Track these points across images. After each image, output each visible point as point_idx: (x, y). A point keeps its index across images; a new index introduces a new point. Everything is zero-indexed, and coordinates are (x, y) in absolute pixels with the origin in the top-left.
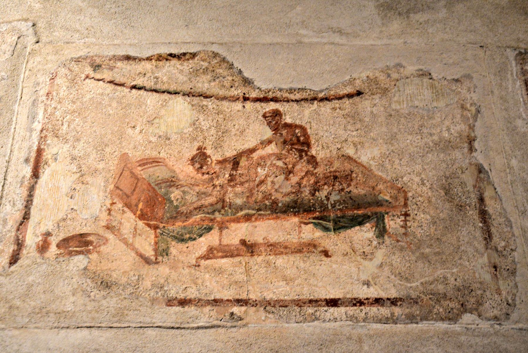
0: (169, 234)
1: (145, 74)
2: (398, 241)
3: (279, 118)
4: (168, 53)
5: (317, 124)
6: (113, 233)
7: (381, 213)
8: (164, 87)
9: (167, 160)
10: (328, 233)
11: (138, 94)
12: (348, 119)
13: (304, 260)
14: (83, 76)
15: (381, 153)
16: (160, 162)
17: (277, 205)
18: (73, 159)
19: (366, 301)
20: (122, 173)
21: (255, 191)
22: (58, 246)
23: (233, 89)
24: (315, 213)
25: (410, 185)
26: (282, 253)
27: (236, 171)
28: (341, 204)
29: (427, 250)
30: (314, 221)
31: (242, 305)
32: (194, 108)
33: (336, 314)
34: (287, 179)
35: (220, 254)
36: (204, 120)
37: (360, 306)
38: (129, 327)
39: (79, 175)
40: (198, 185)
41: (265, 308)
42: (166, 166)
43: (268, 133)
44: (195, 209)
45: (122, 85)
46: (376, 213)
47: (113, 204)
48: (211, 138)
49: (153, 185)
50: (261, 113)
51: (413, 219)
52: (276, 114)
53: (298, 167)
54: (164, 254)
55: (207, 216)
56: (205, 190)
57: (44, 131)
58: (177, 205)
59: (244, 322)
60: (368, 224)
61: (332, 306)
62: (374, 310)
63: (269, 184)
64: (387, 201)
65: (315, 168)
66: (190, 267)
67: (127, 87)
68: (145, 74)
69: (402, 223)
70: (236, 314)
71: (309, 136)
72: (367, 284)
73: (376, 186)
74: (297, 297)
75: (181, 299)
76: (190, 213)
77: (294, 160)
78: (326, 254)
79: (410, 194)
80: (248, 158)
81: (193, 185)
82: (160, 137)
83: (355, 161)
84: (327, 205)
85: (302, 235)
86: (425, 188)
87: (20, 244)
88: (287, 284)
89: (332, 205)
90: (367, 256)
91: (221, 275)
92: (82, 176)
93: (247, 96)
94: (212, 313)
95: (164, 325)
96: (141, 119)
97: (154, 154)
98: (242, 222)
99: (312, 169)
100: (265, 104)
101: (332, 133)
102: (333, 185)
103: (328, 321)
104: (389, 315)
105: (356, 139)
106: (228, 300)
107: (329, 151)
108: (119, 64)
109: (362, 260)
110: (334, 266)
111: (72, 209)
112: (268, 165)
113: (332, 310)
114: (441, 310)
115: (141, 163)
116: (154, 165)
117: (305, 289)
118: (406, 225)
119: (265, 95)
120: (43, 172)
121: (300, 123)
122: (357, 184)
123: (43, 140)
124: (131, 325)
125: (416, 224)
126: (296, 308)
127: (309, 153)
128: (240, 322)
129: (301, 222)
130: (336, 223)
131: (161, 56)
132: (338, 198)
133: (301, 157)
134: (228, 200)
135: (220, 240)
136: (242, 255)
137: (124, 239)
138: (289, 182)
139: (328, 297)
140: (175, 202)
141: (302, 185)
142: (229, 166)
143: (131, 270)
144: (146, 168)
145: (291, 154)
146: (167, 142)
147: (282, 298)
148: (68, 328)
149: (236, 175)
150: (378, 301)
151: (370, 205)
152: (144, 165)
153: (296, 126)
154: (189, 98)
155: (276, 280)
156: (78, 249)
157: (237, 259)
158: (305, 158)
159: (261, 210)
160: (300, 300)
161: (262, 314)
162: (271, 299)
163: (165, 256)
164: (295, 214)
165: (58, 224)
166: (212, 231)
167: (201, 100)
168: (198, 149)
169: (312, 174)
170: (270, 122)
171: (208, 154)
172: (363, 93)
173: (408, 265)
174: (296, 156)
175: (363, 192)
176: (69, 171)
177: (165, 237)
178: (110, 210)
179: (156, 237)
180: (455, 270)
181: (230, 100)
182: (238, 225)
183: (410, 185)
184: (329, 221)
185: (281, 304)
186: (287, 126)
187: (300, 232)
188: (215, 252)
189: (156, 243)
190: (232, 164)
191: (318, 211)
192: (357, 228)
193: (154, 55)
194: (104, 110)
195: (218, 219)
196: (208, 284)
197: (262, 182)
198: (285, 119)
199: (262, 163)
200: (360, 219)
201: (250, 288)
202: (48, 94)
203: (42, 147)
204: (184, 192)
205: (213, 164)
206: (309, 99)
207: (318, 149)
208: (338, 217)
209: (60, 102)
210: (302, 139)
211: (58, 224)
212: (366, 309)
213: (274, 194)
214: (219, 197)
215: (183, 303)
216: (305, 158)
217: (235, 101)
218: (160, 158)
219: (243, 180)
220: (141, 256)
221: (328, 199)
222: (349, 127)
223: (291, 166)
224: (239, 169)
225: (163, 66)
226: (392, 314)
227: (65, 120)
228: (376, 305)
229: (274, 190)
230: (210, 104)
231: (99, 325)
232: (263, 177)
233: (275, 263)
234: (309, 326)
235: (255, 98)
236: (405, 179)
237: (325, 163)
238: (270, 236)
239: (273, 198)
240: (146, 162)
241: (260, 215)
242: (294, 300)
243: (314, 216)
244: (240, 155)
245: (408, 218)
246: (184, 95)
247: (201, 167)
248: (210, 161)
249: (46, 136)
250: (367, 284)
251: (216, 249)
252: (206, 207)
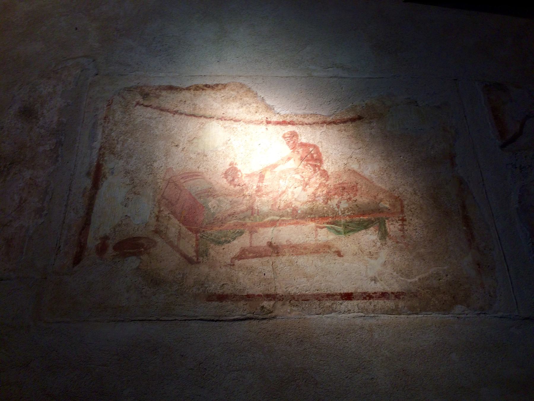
0: (208, 237)
1: (185, 102)
2: (397, 242)
4: (204, 84)
6: (161, 237)
9: (205, 174)
10: (340, 235)
12: (352, 139)
13: (321, 260)
14: (134, 103)
15: (380, 167)
17: (297, 212)
18: (127, 172)
19: (374, 295)
20: (168, 184)
21: (278, 201)
22: (115, 248)
23: (257, 114)
24: (328, 218)
25: (405, 194)
26: (302, 254)
27: (262, 182)
28: (349, 211)
29: (422, 250)
30: (328, 225)
31: (271, 300)
32: (226, 129)
33: (350, 307)
34: (304, 190)
35: (251, 255)
37: (370, 299)
38: (176, 320)
39: (131, 186)
40: (231, 195)
41: (290, 302)
42: (204, 178)
43: (287, 151)
44: (229, 215)
45: (168, 111)
46: (378, 219)
47: (160, 211)
49: (194, 195)
50: (281, 134)
51: (409, 223)
52: (294, 135)
53: (313, 180)
54: (204, 255)
55: (239, 221)
56: (237, 199)
57: (103, 149)
59: (273, 314)
60: (372, 228)
61: (346, 299)
62: (381, 303)
63: (290, 194)
64: (387, 208)
65: (327, 181)
66: (226, 266)
67: (171, 112)
68: (185, 102)
69: (400, 227)
70: (265, 308)
71: (321, 154)
72: (375, 280)
74: (316, 292)
75: (219, 295)
77: (310, 174)
78: (339, 254)
79: (405, 203)
80: (271, 171)
81: (227, 195)
82: (199, 154)
83: (360, 175)
84: (338, 211)
85: (318, 238)
86: (417, 197)
87: (82, 247)
88: (308, 280)
89: (342, 211)
91: (252, 273)
92: (134, 187)
93: (269, 120)
94: (245, 306)
95: (205, 318)
98: (268, 227)
99: (324, 181)
102: (342, 195)
103: (343, 313)
104: (394, 307)
105: (359, 156)
106: (259, 295)
108: (164, 93)
109: (369, 259)
110: (346, 264)
111: (126, 216)
112: (288, 178)
113: (346, 303)
114: (437, 302)
115: (183, 176)
116: (194, 178)
117: (323, 284)
118: (404, 228)
119: (284, 119)
120: (102, 184)
122: (362, 194)
123: (101, 156)
124: (177, 318)
125: (411, 228)
126: (316, 301)
127: (321, 168)
128: (269, 315)
129: (317, 227)
130: (346, 228)
131: (198, 87)
132: (346, 206)
133: (315, 171)
134: (256, 208)
135: (251, 243)
136: (270, 256)
137: (170, 241)
138: (305, 193)
139: (342, 292)
140: (212, 209)
141: (317, 195)
142: (256, 179)
143: (177, 270)
145: (307, 169)
146: (205, 158)
147: (304, 292)
148: (123, 321)
149: (262, 186)
150: (384, 295)
153: (310, 145)
155: (298, 277)
156: (131, 251)
157: (266, 259)
158: (319, 172)
159: (283, 216)
160: (319, 295)
161: (288, 308)
162: (295, 293)
163: (205, 257)
164: (313, 220)
165: (115, 229)
166: (244, 235)
167: (232, 124)
168: (230, 165)
169: (325, 186)
170: (289, 142)
171: (239, 169)
173: (407, 263)
176: (123, 183)
177: (205, 240)
178: (158, 218)
179: (197, 240)
180: (445, 268)
182: (266, 229)
183: (405, 194)
184: (340, 226)
185: (303, 298)
186: (303, 145)
187: (317, 235)
188: (247, 253)
189: (197, 245)
190: (258, 177)
191: (331, 217)
192: (364, 231)
193: (192, 86)
194: (152, 132)
195: (249, 224)
196: (241, 281)
197: (284, 192)
199: (284, 176)
200: (365, 224)
201: (277, 284)
202: (105, 117)
203: (101, 162)
204: (219, 200)
205: (243, 177)
206: (320, 122)
207: (329, 164)
208: (347, 222)
209: (115, 125)
210: (315, 156)
211: (115, 229)
212: (374, 302)
213: (294, 202)
214: (248, 205)
215: (222, 298)
216: (319, 172)
217: (259, 124)
218: (199, 172)
219: (268, 191)
220: (185, 257)
221: (338, 207)
222: (353, 146)
223: (306, 179)
224: (264, 181)
225: (200, 95)
226: (397, 306)
227: (120, 140)
228: (382, 298)
229: (294, 199)
230: (239, 126)
231: (150, 318)
232: (284, 189)
233: (297, 262)
234: (328, 317)
235: (276, 122)
236: (400, 189)
237: (335, 176)
238: (292, 239)
239: (293, 206)
241: (283, 220)
242: (314, 295)
243: (328, 221)
244: (265, 170)
245: (405, 223)
246: (217, 119)
247: (233, 180)
249: (104, 154)
250: (374, 280)
251: (247, 250)
252: (238, 214)
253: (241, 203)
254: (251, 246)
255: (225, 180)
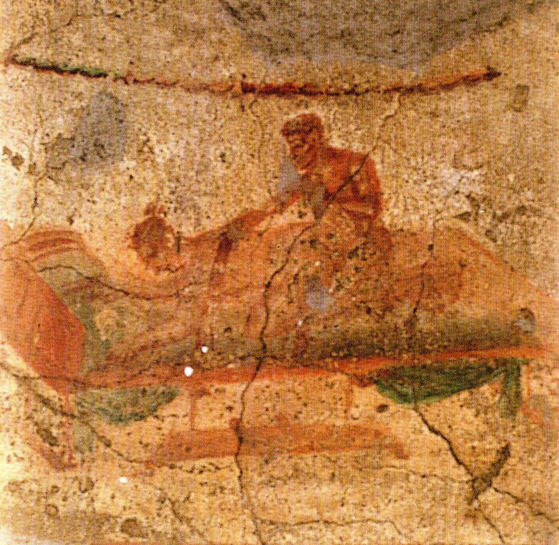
0: (93, 404)
3: (316, 137)
5: (395, 151)
7: (514, 361)
8: (75, 63)
9: (85, 237)
10: (406, 405)
11: (21, 77)
16: (70, 241)
23: (220, 64)
27: (225, 262)
36: (159, 142)
42: (83, 249)
44: (143, 348)
46: (505, 362)
48: (173, 185)
49: (57, 292)
50: (280, 124)
52: (311, 126)
58: (107, 340)
71: (378, 182)
73: (511, 300)
76: (132, 358)
85: (354, 412)
90: (479, 455)
93: (250, 81)
96: (31, 138)
97: (61, 222)
100: (288, 102)
101: (428, 173)
107: (417, 218)
115: (34, 242)
119: (290, 79)
121: (361, 150)
134: (208, 331)
140: (102, 333)
142: (210, 251)
144: (42, 256)
151: (495, 343)
152: (41, 248)
154: (126, 87)
166: (177, 401)
168: (147, 212)
170: (298, 146)
172: (499, 74)
174: (348, 230)
175: (481, 313)
181: (213, 92)
186: (333, 155)
198: (328, 140)
207: (396, 212)
210: (363, 188)
214: (189, 323)
218: (71, 233)
219: (237, 285)
240: (41, 239)
247: (154, 255)
248: (173, 240)
253: (172, 317)
254: (193, 430)
255: (134, 254)
